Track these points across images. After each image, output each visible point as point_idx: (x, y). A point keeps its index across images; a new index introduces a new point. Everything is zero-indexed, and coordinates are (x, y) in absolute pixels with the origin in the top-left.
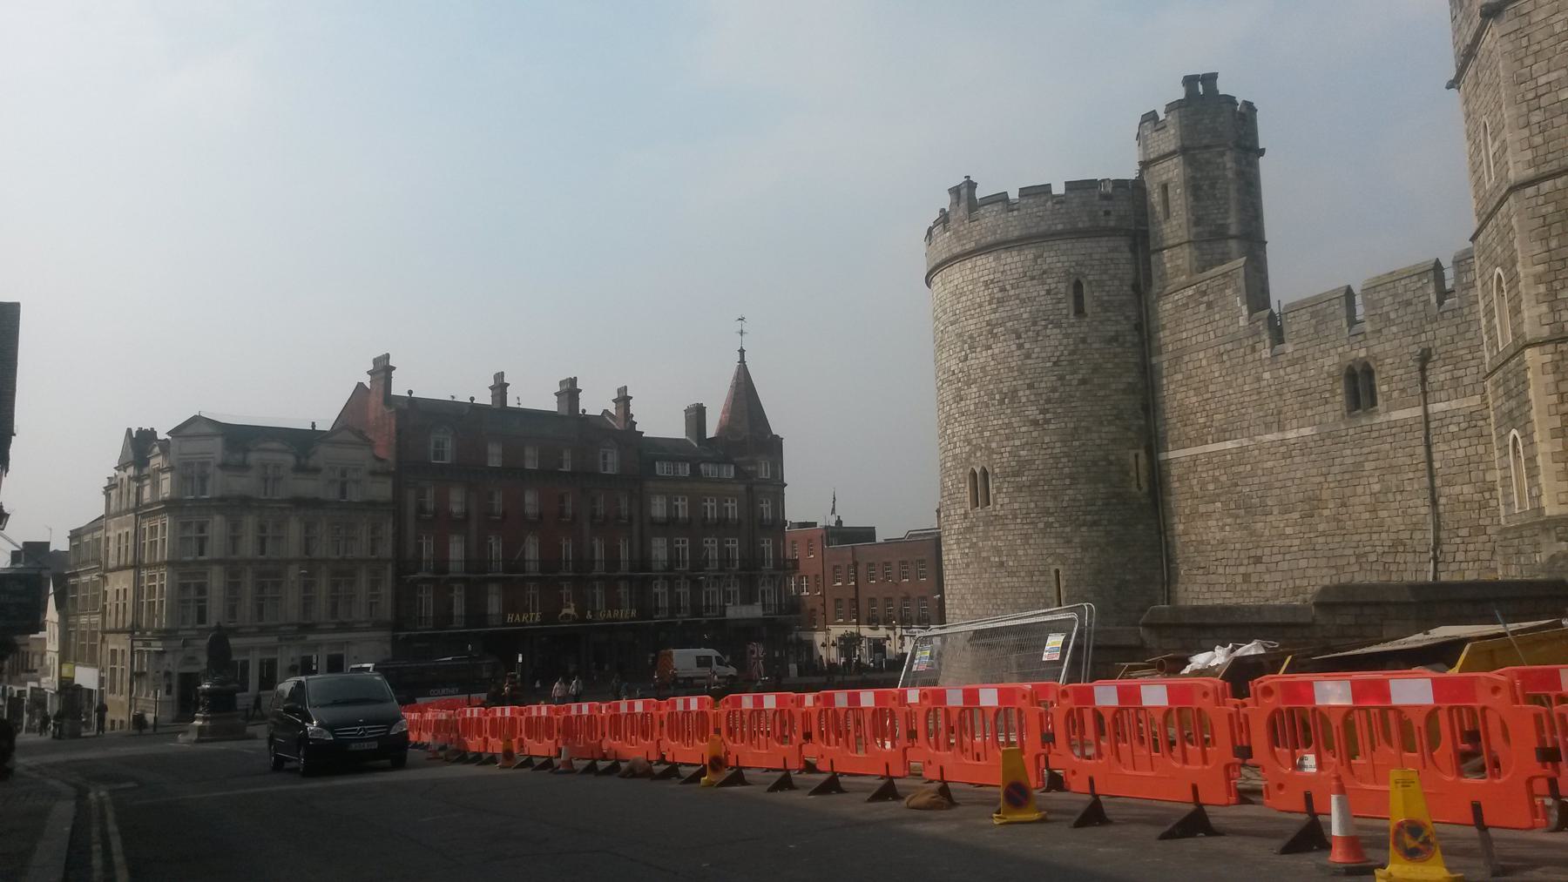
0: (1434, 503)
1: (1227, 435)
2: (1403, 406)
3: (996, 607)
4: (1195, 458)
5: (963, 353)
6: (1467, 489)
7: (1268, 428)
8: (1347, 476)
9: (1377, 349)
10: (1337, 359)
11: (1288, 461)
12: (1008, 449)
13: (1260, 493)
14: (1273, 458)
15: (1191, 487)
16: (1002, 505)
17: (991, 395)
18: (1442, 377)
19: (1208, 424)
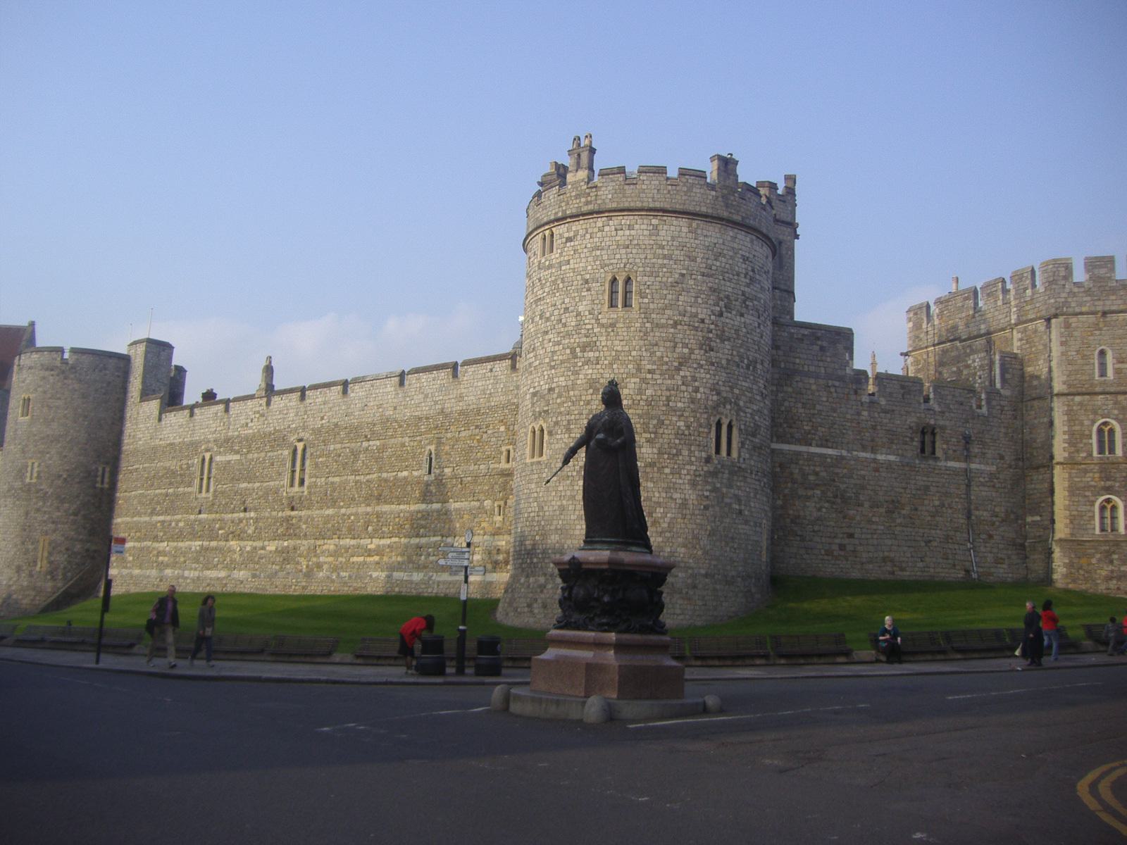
0: (969, 518)
1: (830, 444)
2: (954, 459)
3: (733, 550)
4: (799, 453)
5: (718, 309)
6: (985, 514)
7: (864, 449)
8: (919, 492)
9: (941, 423)
10: (914, 419)
11: (877, 474)
12: (750, 411)
13: (854, 491)
14: (866, 469)
15: (792, 474)
16: (744, 459)
17: (741, 357)
18: (976, 450)
19: (813, 432)
